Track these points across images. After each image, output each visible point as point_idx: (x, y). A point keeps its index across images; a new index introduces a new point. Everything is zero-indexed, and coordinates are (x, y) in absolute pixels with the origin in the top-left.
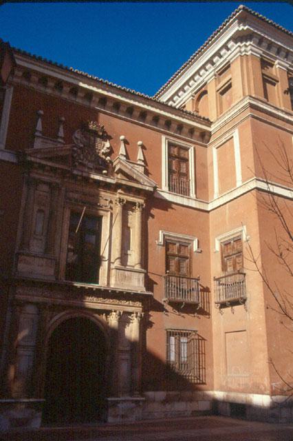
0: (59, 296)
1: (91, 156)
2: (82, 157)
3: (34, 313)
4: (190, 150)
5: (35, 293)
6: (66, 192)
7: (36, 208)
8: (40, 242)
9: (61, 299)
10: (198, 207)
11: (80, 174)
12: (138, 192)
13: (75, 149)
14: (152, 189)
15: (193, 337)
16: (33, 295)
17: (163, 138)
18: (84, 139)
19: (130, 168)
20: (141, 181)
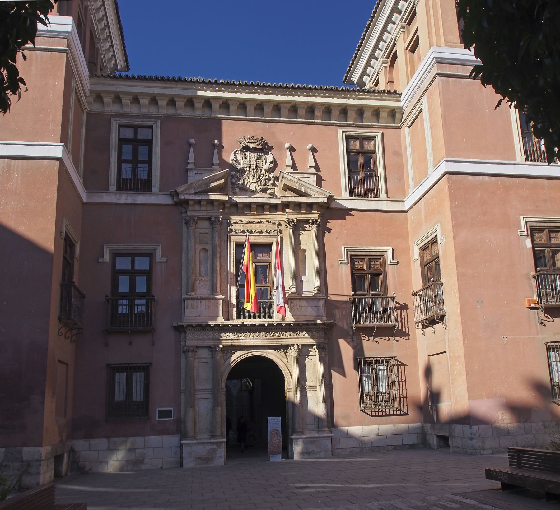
0: (231, 338)
3: (209, 356)
4: (376, 139)
5: (206, 337)
7: (199, 247)
8: (206, 283)
9: (232, 339)
10: (390, 209)
12: (310, 207)
13: (233, 173)
14: (325, 200)
15: (393, 363)
16: (204, 340)
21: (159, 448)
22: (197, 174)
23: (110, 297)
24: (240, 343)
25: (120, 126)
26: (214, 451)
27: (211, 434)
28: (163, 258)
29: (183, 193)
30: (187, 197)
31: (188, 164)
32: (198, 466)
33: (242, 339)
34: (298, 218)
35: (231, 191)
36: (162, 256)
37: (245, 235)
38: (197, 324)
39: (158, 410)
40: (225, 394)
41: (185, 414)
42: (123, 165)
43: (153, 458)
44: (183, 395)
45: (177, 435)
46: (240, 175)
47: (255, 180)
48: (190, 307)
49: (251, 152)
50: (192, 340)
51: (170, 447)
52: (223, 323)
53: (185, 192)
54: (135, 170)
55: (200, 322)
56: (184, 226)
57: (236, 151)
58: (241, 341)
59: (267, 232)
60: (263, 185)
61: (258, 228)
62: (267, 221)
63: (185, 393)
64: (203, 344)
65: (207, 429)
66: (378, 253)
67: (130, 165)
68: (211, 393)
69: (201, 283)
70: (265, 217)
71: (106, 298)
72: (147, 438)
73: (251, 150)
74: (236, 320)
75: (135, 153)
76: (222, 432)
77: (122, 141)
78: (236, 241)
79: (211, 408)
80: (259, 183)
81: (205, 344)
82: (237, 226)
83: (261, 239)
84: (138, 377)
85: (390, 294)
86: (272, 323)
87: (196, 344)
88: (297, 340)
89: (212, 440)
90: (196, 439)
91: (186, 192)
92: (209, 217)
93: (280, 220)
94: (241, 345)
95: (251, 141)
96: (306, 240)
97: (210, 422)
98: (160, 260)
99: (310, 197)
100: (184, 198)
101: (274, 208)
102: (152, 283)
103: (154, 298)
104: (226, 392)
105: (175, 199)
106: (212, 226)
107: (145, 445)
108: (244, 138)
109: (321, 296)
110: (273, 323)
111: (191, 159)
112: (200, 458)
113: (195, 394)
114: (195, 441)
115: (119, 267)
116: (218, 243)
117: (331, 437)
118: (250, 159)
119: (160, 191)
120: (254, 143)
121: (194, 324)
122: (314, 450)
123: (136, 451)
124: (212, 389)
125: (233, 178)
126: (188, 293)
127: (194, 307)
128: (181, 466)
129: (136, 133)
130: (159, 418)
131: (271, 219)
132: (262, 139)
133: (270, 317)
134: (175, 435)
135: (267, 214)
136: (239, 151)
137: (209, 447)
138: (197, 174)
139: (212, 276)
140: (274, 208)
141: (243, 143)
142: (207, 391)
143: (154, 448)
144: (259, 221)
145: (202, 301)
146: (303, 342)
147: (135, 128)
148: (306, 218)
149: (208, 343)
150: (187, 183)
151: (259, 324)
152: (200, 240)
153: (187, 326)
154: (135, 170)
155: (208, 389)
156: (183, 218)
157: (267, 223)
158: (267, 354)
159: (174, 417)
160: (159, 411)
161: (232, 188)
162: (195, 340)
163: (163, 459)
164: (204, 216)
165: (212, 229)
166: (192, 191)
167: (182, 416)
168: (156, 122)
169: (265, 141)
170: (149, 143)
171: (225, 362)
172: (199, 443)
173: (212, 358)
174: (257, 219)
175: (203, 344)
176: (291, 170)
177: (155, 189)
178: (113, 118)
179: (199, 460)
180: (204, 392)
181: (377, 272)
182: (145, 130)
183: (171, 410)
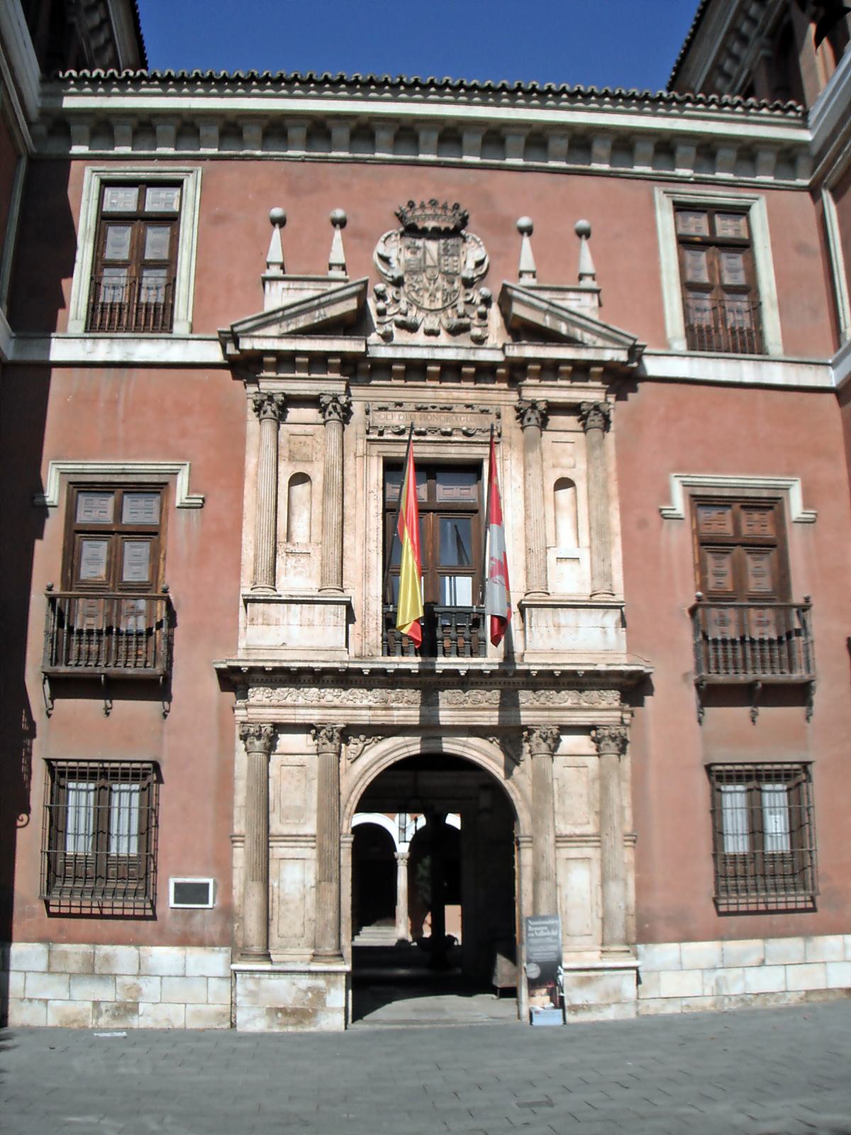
0: (365, 703)
1: (432, 295)
2: (403, 306)
3: (309, 752)
6: (367, 412)
8: (303, 560)
9: (370, 708)
10: (794, 382)
14: (622, 356)
17: (658, 192)
18: (408, 255)
19: (545, 306)
20: (587, 337)
21: (176, 976)
22: (288, 289)
23: (57, 590)
24: (392, 718)
25: (106, 184)
26: (319, 995)
27: (312, 951)
28: (195, 496)
29: (248, 333)
31: (268, 265)
32: (276, 1030)
33: (399, 709)
34: (550, 400)
36: (191, 490)
37: (405, 441)
38: (277, 665)
39: (172, 882)
40: (350, 850)
41: (244, 896)
42: (106, 272)
43: (161, 1002)
44: (240, 847)
45: (224, 949)
46: (397, 293)
47: (439, 305)
48: (260, 621)
49: (429, 238)
50: (264, 706)
51: (204, 976)
52: (346, 665)
54: (135, 285)
55: (285, 661)
56: (252, 416)
57: (389, 236)
58: (396, 713)
59: (466, 434)
60: (459, 317)
61: (445, 422)
62: (468, 406)
63: (243, 841)
64: (293, 717)
65: (303, 937)
66: (765, 494)
67: (125, 272)
68: (313, 844)
69: (292, 561)
70: (462, 395)
71: (49, 593)
72: (145, 950)
73: (428, 235)
74: (382, 659)
75: (139, 245)
76: (339, 947)
77: (106, 219)
78: (385, 455)
79: (313, 883)
80: (450, 311)
81: (297, 717)
82: (389, 417)
83: (453, 451)
84: (126, 800)
85: (797, 598)
86: (477, 667)
87: (275, 717)
88: (546, 713)
89: (315, 967)
90: (271, 961)
92: (316, 393)
93: (503, 403)
94: (395, 723)
95: (429, 212)
96: (571, 456)
97: (310, 920)
98: (187, 501)
99: (582, 347)
101: (485, 372)
102: (164, 559)
103: (168, 597)
104: (354, 843)
105: (231, 349)
106: (324, 417)
107: (140, 968)
109: (611, 600)
110: (483, 667)
111: (275, 252)
112: (283, 1011)
113: (272, 847)
114: (267, 967)
115: (83, 518)
116: (338, 459)
117: (636, 968)
118: (425, 253)
119: (191, 332)
120: (434, 217)
121: (269, 666)
122: (591, 1002)
123: (118, 980)
124: (315, 836)
126: (256, 584)
127: (271, 622)
128: (233, 1025)
129: (142, 199)
130: (176, 901)
131: (478, 402)
132: (456, 207)
133: (472, 654)
134: (217, 948)
135: (467, 389)
136: (397, 235)
137: (305, 982)
138: (288, 289)
139: (321, 543)
140: (485, 372)
142: (304, 839)
143: (162, 977)
144: (448, 406)
145: (293, 606)
146: (564, 719)
147: (143, 185)
148: (573, 401)
149: (308, 717)
151: (444, 670)
152: (290, 451)
153: (252, 669)
154: (135, 285)
155: (305, 836)
156: (250, 396)
157: (469, 410)
158: (466, 750)
159: (214, 902)
160: (177, 886)
162: (273, 706)
163: (185, 1004)
164: (302, 393)
165: (324, 424)
167: (236, 902)
168: (191, 172)
170: (170, 220)
171: (351, 767)
172: (279, 972)
173: (318, 754)
174: (442, 401)
175: (293, 717)
177: (181, 327)
178: (89, 167)
179: (280, 1015)
180: (296, 841)
181: (762, 542)
182: (163, 193)
183: (207, 885)
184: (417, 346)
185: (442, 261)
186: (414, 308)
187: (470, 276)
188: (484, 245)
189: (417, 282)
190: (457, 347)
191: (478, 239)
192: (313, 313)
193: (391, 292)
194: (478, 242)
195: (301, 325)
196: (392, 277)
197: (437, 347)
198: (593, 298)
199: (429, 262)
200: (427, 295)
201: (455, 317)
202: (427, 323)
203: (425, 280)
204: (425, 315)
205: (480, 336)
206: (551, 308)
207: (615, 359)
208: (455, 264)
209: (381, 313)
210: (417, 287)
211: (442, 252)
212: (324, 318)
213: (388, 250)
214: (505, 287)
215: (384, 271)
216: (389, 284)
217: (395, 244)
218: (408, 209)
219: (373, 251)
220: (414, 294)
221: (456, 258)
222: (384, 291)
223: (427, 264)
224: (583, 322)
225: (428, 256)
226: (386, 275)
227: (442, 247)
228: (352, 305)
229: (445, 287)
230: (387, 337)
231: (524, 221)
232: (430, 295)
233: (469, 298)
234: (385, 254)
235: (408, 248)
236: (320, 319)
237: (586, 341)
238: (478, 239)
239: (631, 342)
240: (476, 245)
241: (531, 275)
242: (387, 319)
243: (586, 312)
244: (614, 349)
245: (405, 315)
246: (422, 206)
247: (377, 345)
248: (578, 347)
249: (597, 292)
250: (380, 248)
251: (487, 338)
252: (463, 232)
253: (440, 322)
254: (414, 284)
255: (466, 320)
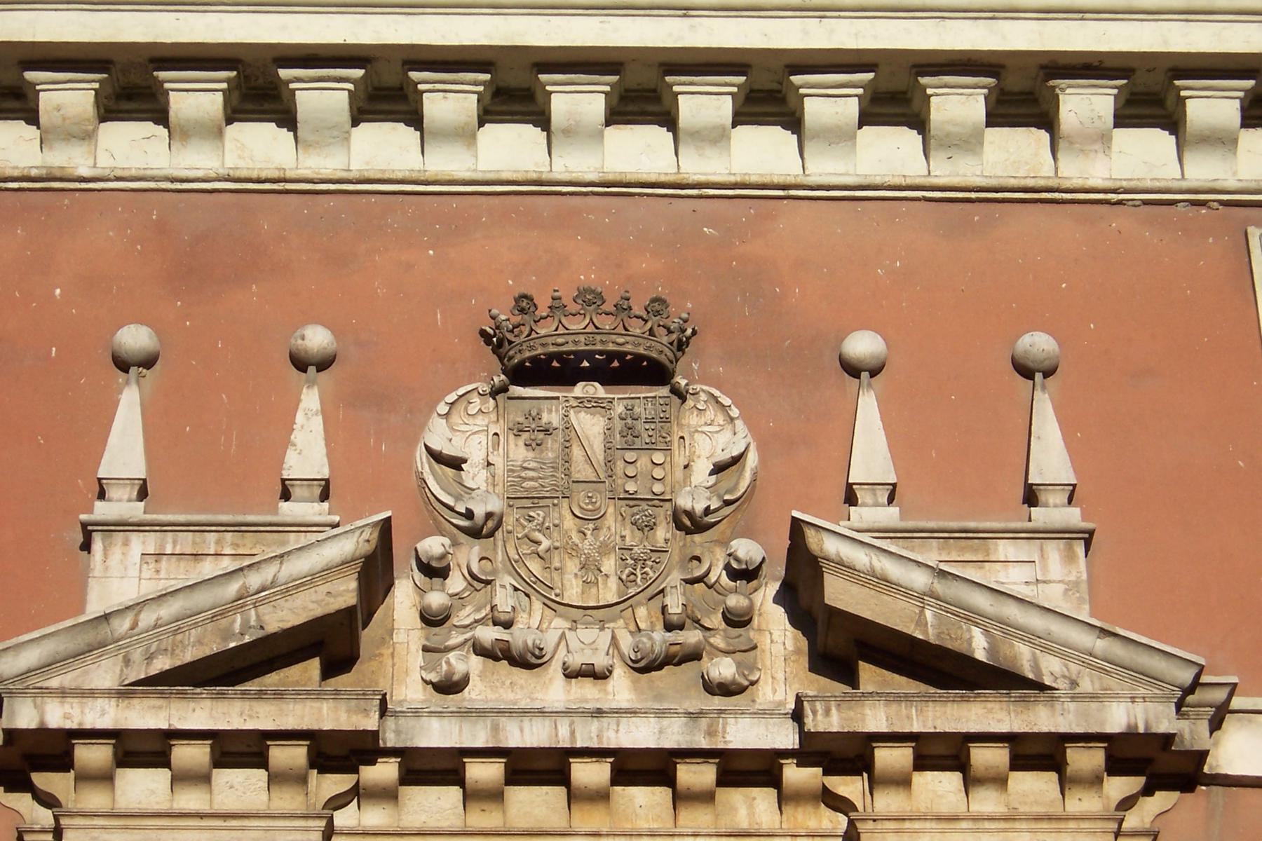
1: (590, 567)
11: (480, 740)
14: (1163, 720)
18: (519, 452)
19: (920, 579)
20: (1051, 668)
22: (159, 555)
30: (57, 716)
35: (415, 676)
47: (609, 592)
53: (45, 684)
60: (669, 627)
91: (54, 683)
100: (42, 722)
108: (524, 304)
118: (567, 446)
125: (437, 581)
132: (658, 305)
138: (159, 555)
141: (517, 341)
150: (82, 611)
161: (426, 649)
166: (105, 674)
169: (685, 321)
176: (889, 515)
184: (541, 712)
185: (620, 464)
186: (537, 605)
187: (699, 508)
188: (742, 416)
189: (542, 529)
190: (661, 713)
191: (726, 401)
192: (224, 622)
193: (470, 554)
194: (723, 407)
195: (189, 656)
196: (469, 515)
197: (599, 713)
198: (1070, 558)
199: (582, 470)
200: (572, 566)
201: (660, 625)
202: (574, 644)
203: (569, 523)
204: (567, 625)
205: (734, 682)
206: (940, 587)
207: (1141, 730)
208: (658, 473)
209: (431, 619)
210: (546, 543)
211: (618, 440)
212: (260, 634)
213: (458, 440)
214: (797, 527)
215: (449, 500)
216: (463, 538)
217: (481, 421)
218: (517, 319)
219: (416, 441)
220: (535, 566)
221: (658, 457)
222: (443, 557)
223: (576, 476)
224: (1036, 621)
225: (577, 452)
226: (451, 509)
227: (618, 425)
228: (345, 593)
229: (628, 542)
230: (449, 686)
231: (863, 345)
232: (583, 567)
233: (697, 573)
234: (448, 450)
235: (519, 431)
236: (247, 639)
237: (1048, 681)
238: (726, 401)
239: (1186, 676)
240: (720, 419)
241: (884, 498)
242: (456, 639)
243: (1052, 596)
244: (1133, 699)
245: (508, 625)
246: (557, 306)
247: (416, 713)
248: (1023, 699)
249: (1088, 538)
250: (438, 436)
251: (753, 683)
252: (683, 382)
253: (614, 641)
254: (538, 536)
255: (691, 637)
